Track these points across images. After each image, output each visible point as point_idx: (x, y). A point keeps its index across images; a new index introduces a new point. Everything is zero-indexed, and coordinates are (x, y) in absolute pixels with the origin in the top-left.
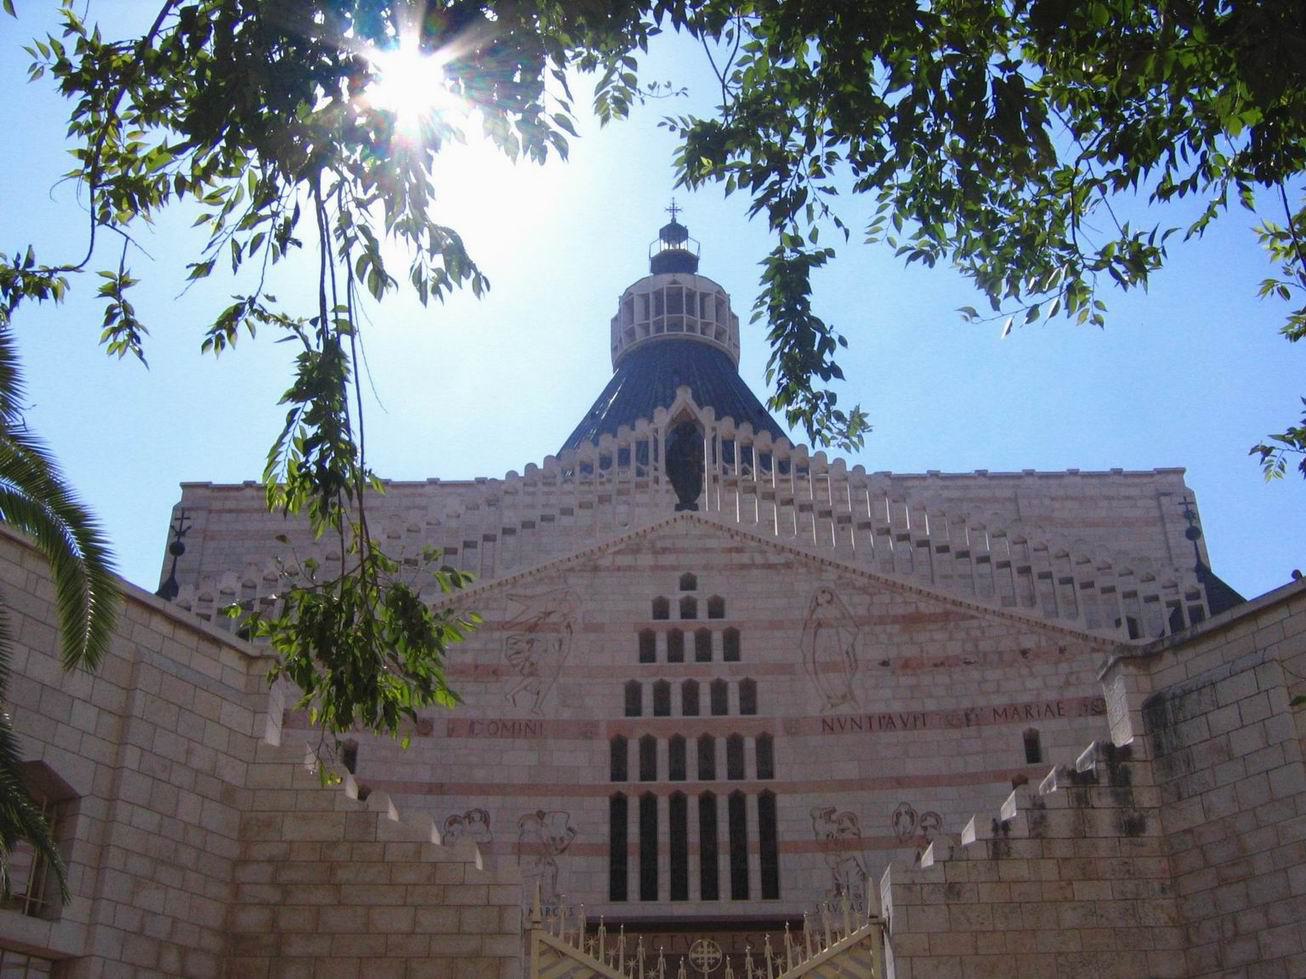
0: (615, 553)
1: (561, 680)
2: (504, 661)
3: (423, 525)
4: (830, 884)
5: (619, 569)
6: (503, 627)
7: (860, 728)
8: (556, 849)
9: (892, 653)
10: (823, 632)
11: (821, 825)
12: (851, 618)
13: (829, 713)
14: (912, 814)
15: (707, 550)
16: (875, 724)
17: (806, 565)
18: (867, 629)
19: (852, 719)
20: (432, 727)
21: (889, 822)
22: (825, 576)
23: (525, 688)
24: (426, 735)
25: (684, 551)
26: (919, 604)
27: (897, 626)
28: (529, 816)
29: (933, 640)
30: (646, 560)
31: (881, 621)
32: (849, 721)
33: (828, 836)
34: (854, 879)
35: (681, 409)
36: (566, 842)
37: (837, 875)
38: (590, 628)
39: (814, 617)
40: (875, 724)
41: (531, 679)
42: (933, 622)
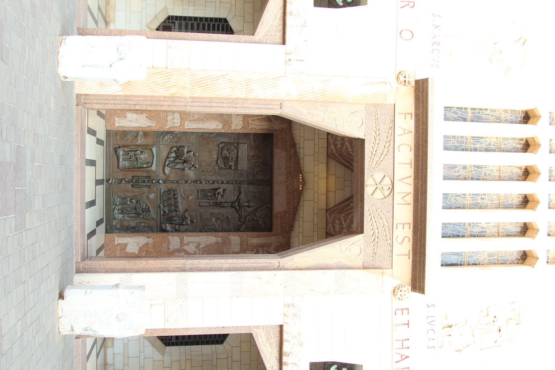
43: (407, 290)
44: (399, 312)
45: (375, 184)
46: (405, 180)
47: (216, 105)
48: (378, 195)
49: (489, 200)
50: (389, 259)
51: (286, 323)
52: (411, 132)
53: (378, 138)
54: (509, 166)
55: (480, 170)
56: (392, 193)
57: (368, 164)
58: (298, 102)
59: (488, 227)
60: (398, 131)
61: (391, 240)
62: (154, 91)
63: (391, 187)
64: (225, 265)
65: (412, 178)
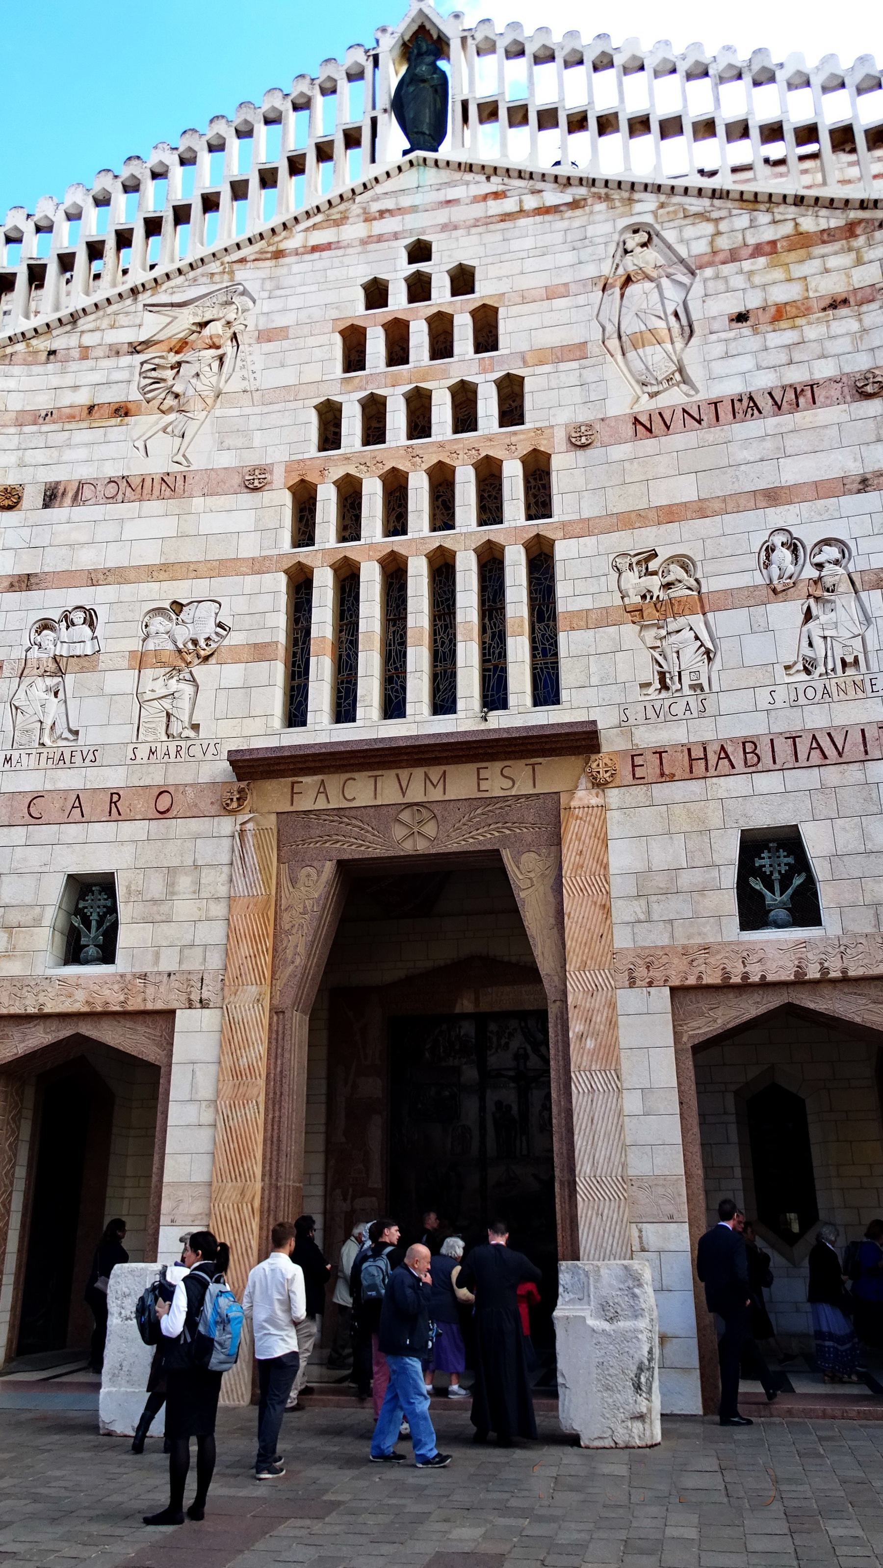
0: (307, 230)
1: (218, 412)
2: (135, 395)
3: (28, 228)
4: (649, 674)
5: (315, 249)
6: (135, 348)
7: (699, 422)
8: (198, 657)
9: (753, 301)
10: (631, 289)
11: (633, 581)
12: (682, 261)
13: (646, 405)
14: (793, 547)
15: (449, 202)
16: (725, 410)
17: (607, 198)
18: (709, 272)
19: (684, 411)
20: (19, 498)
21: (754, 564)
22: (638, 207)
23: (164, 430)
24: (10, 508)
25: (414, 209)
26: (800, 220)
27: (762, 261)
28: (159, 611)
29: (827, 271)
30: (354, 230)
31: (734, 256)
32: (679, 413)
33: (644, 597)
34: (691, 658)
35: (415, 27)
36: (214, 646)
37: (660, 659)
38: (266, 336)
39: (621, 271)
40: (725, 410)
41: (172, 416)
42: (824, 242)
43: (597, 763)
44: (639, 772)
45: (411, 838)
46: (404, 785)
47: (276, 1131)
48: (430, 829)
49: (444, 633)
50: (541, 801)
51: (666, 981)
52: (323, 781)
53: (335, 837)
54: (388, 606)
55: (393, 654)
56: (427, 805)
57: (378, 851)
58: (274, 982)
59: (492, 629)
60: (321, 804)
61: (510, 798)
62: (247, 1250)
63: (416, 808)
64: (562, 1103)
65: (399, 771)
